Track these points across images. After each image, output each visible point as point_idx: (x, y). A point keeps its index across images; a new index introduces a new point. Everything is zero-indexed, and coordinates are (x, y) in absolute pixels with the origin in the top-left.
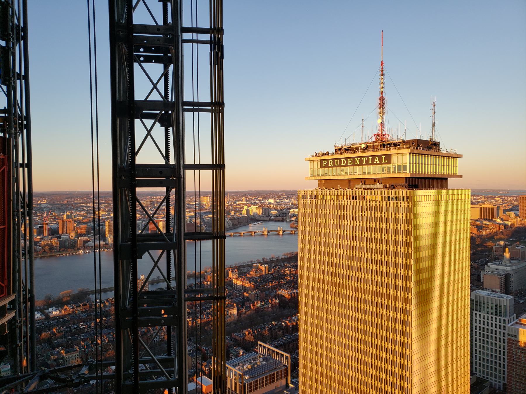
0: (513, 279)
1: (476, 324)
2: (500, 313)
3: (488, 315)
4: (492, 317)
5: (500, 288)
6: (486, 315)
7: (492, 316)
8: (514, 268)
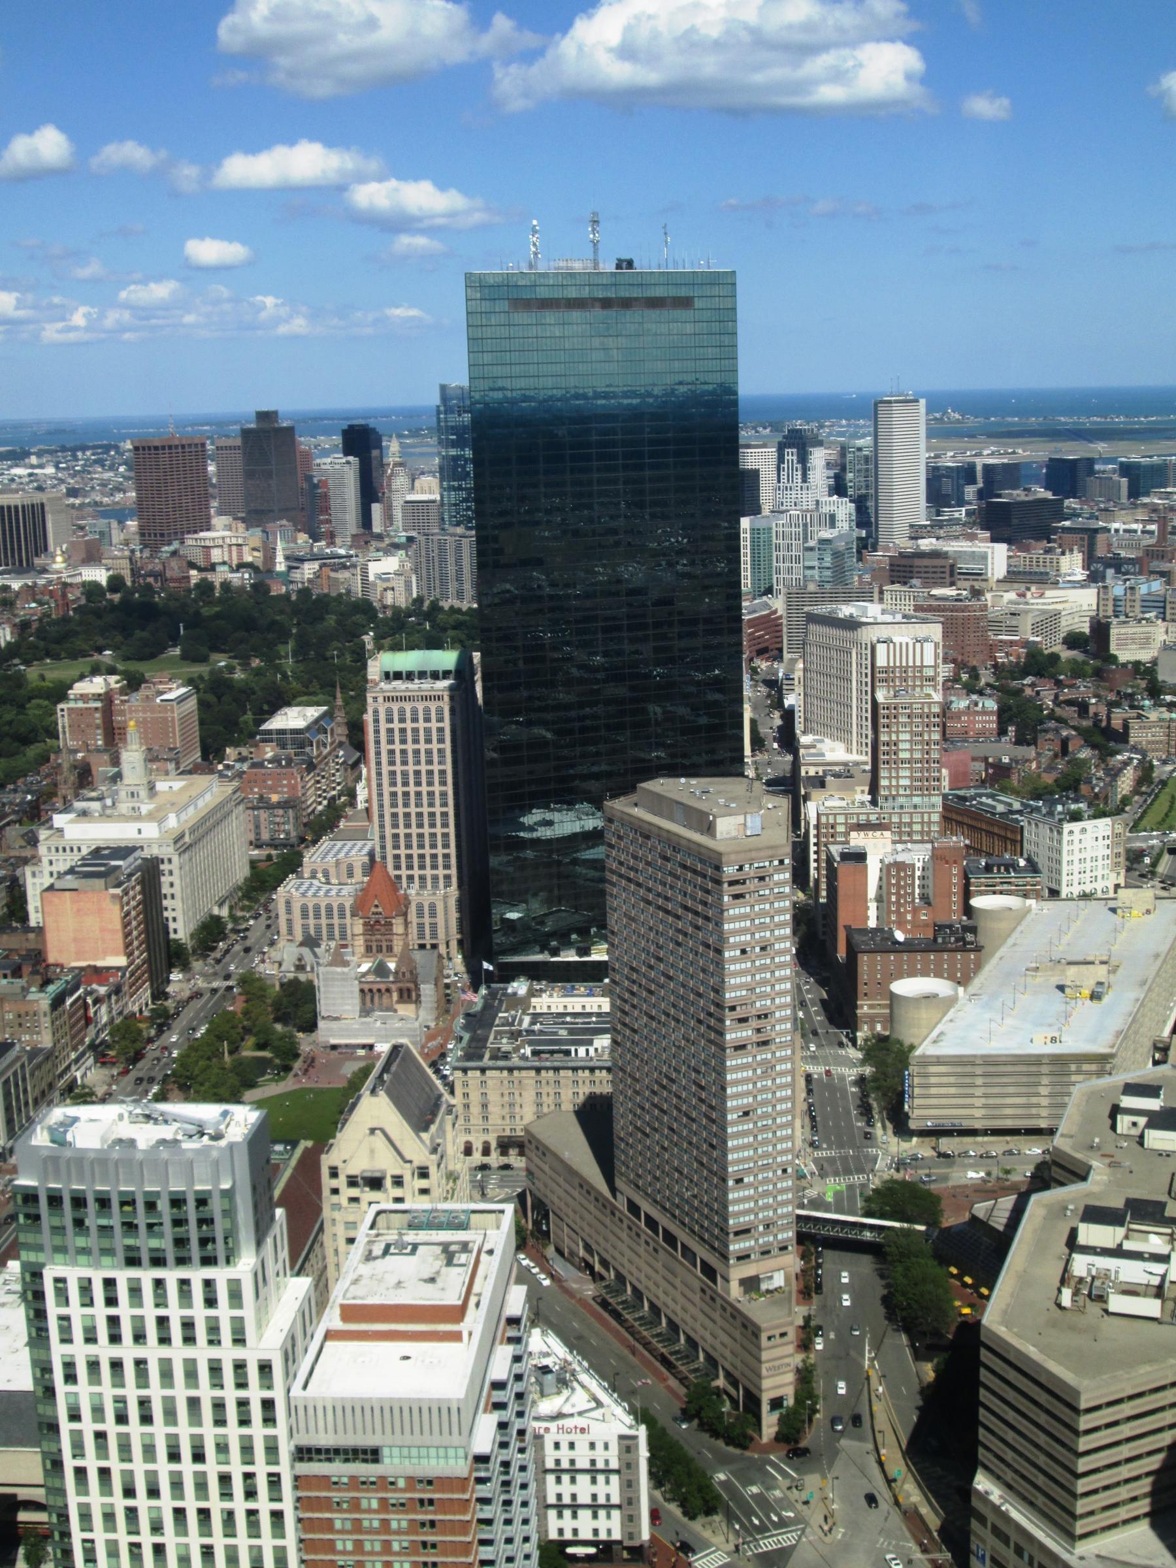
0: (173, 883)
1: (67, 1349)
2: (204, 1242)
3: (133, 1273)
4: (159, 1283)
5: (127, 945)
6: (123, 1276)
7: (159, 1273)
8: (172, 822)
